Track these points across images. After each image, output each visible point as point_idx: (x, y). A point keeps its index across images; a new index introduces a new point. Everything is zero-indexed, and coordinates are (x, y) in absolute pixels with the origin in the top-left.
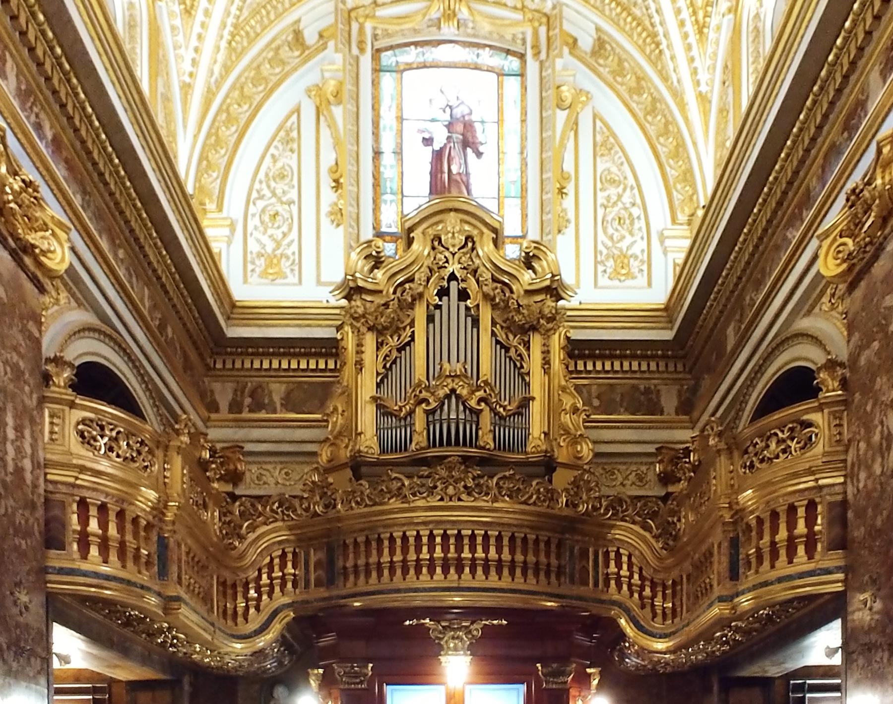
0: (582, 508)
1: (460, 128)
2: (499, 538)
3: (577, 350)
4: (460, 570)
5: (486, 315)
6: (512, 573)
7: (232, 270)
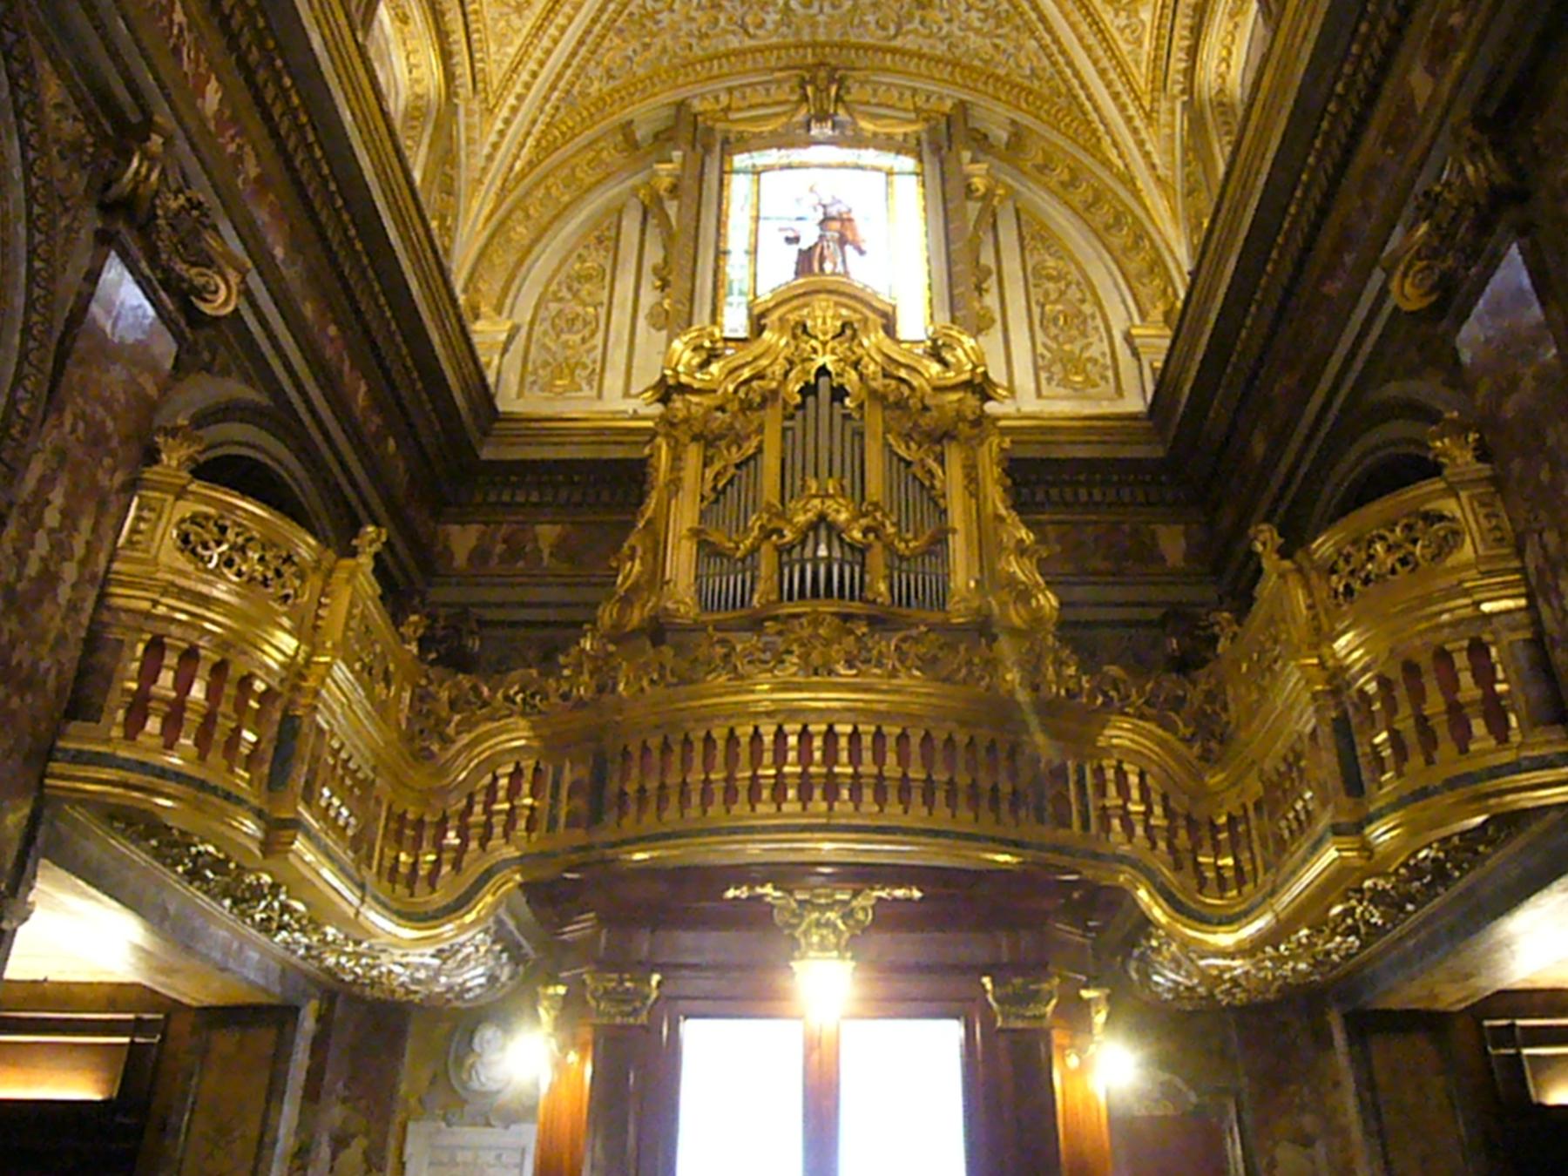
2: (903, 738)
4: (831, 794)
6: (928, 801)
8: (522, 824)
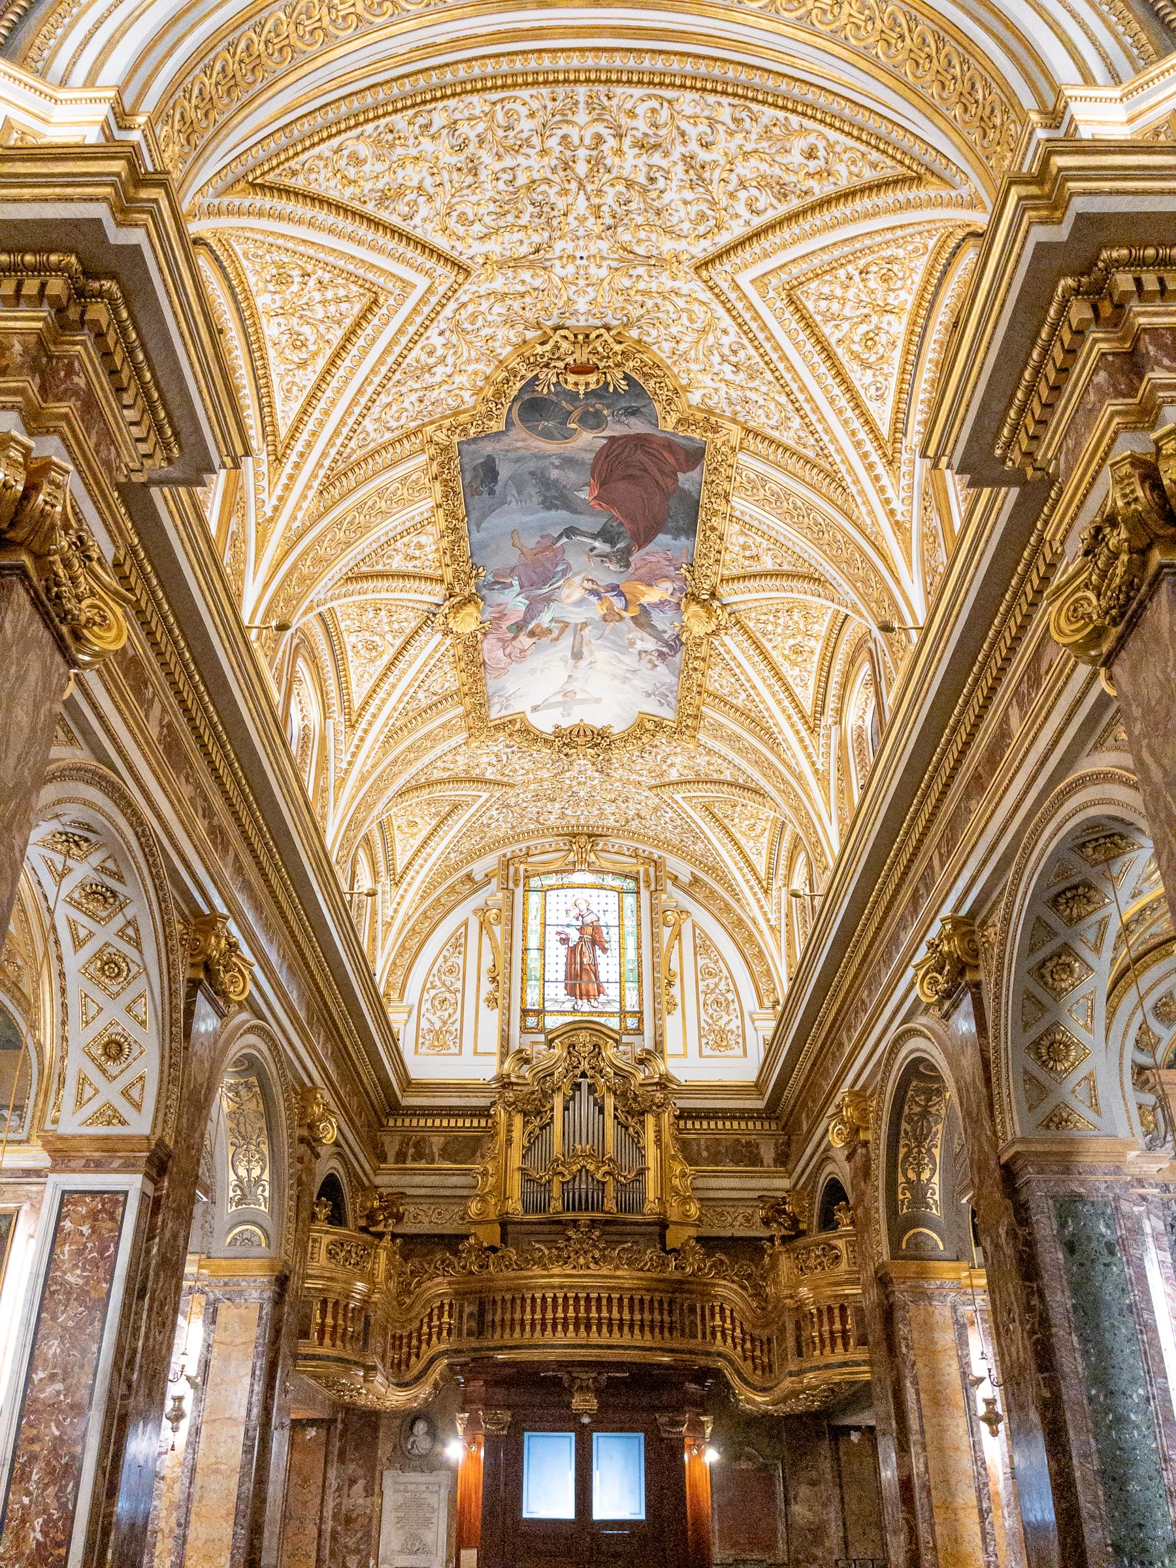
0: (688, 1270)
1: (590, 930)
2: (621, 1299)
3: (685, 1115)
4: (588, 1328)
5: (610, 1102)
7: (407, 1044)
8: (445, 1333)
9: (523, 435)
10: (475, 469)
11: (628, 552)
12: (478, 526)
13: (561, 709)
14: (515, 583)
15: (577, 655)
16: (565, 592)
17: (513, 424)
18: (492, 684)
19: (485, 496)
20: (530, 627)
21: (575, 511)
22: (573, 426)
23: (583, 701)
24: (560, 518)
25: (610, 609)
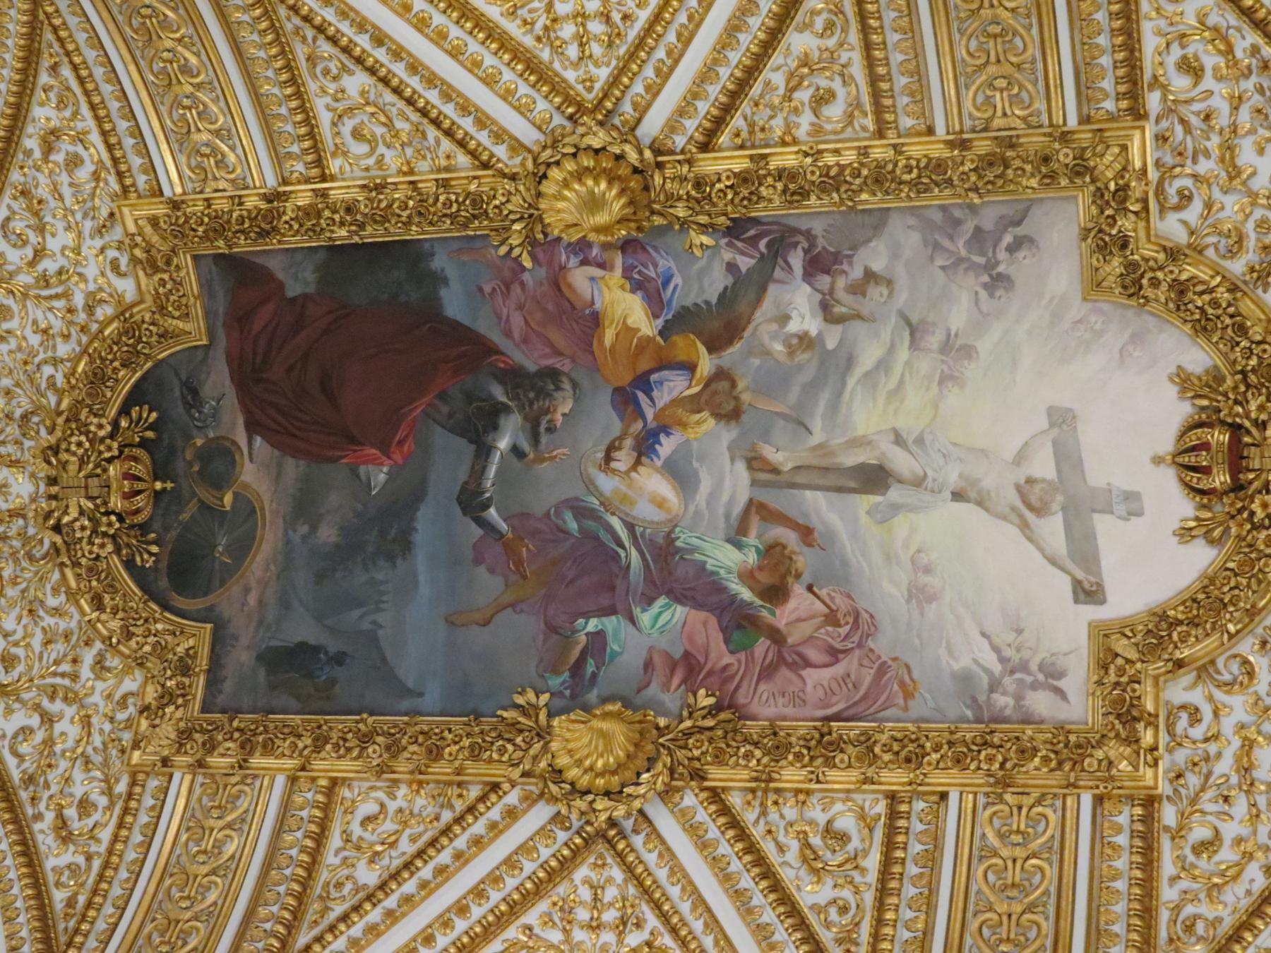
9: (236, 590)
10: (273, 687)
11: (513, 377)
12: (407, 692)
13: (1107, 529)
14: (593, 625)
15: (874, 478)
16: (645, 511)
17: (211, 609)
18: (935, 704)
19: (339, 672)
20: (746, 594)
21: (418, 495)
22: (228, 499)
23: (1068, 456)
24: (431, 523)
25: (695, 404)
